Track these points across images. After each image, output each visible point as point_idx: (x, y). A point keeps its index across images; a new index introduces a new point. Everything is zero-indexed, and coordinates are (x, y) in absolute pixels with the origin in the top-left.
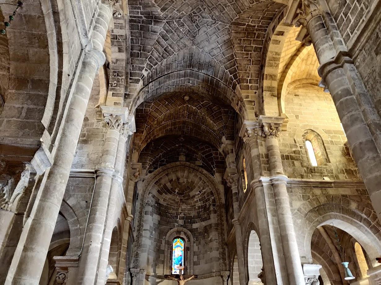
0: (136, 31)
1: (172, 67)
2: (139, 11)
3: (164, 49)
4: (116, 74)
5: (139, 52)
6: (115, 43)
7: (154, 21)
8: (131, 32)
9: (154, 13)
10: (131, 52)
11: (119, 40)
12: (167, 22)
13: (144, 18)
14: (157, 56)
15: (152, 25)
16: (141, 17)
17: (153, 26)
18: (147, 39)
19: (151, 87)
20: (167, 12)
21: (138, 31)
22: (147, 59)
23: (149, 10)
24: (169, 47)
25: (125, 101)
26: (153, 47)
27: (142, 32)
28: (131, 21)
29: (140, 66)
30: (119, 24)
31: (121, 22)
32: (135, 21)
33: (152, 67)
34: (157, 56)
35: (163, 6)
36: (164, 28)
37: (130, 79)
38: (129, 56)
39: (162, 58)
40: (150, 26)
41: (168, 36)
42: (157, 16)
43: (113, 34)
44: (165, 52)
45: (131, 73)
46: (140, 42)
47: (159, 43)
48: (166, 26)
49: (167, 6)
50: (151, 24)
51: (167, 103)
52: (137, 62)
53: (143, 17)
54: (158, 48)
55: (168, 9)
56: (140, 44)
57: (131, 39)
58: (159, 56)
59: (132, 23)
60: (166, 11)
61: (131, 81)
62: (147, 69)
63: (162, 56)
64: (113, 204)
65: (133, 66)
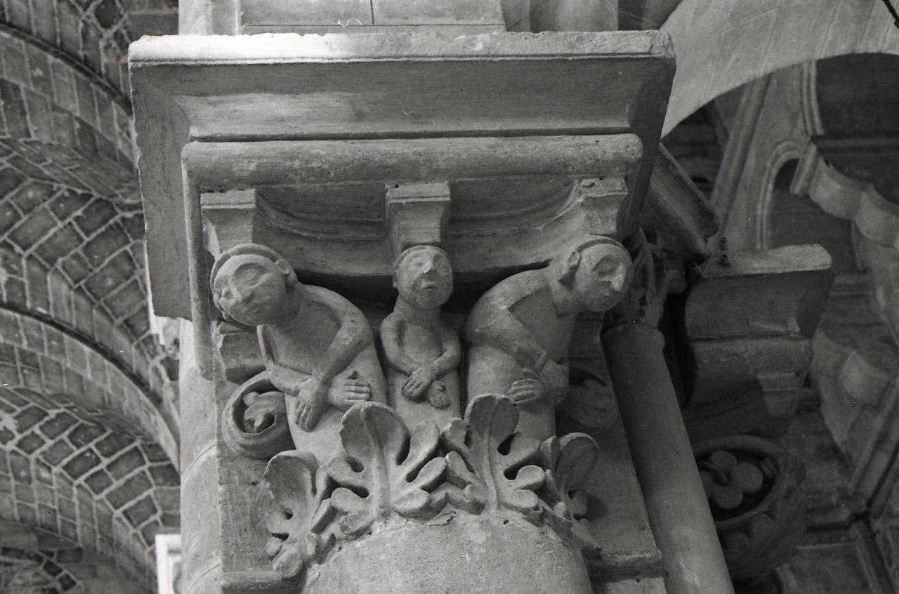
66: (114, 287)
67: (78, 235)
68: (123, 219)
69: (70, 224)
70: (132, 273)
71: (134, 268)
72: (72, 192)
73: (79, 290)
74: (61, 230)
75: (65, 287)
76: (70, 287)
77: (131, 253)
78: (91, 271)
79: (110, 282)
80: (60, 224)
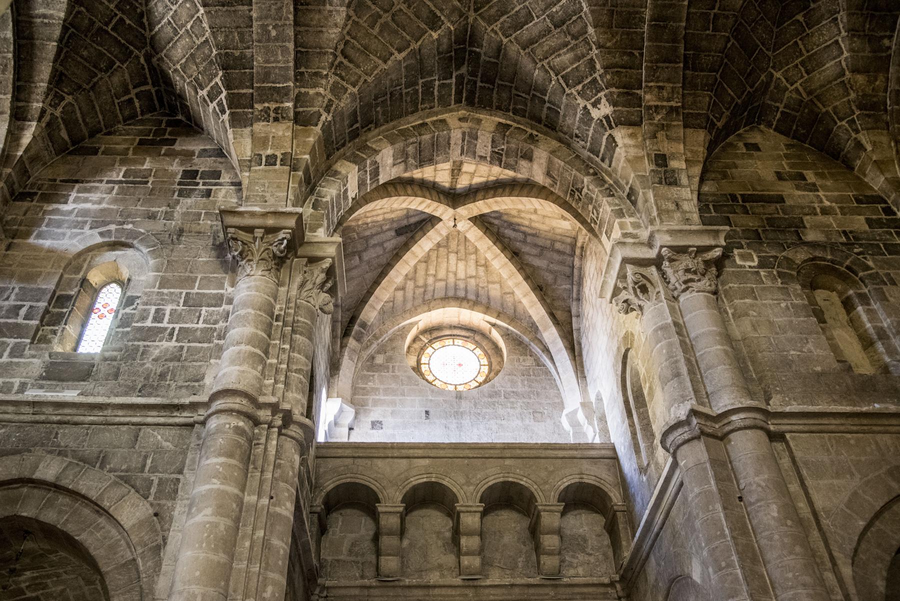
0: (495, 95)
1: (627, 5)
2: (437, 83)
3: (556, 27)
4: (577, 193)
5: (547, 105)
6: (511, 161)
7: (471, 45)
8: (499, 108)
9: (445, 47)
10: (545, 125)
11: (503, 150)
12: (476, 10)
13: (464, 70)
14: (570, 56)
15: (482, 52)
16: (460, 78)
17: (485, 50)
18: (515, 73)
19: (661, 99)
20: (441, 10)
21: (495, 92)
22: (568, 91)
23: (432, 62)
24: (554, 10)
25: (638, 211)
26: (539, 65)
27: (498, 81)
28: (471, 103)
29: (581, 119)
30: (463, 140)
31: (460, 136)
32: (471, 94)
33: (595, 80)
34: (570, 56)
35: (423, 26)
36: (491, 21)
37: (603, 160)
38: (553, 133)
39: (581, 39)
40: (483, 57)
41: (517, 9)
42: (453, 37)
43: (488, 159)
44: (564, 27)
45: (591, 150)
46: (523, 95)
47: (532, 42)
48: (486, 15)
49: (425, 13)
50: (478, 55)
51: (800, 17)
52: (569, 121)
53: (459, 72)
54: (546, 48)
55: (433, 8)
56: (527, 96)
57: (514, 114)
58: (572, 49)
59: (476, 100)
60: (439, 14)
61: (607, 161)
62: (593, 100)
63: (577, 39)
64: (758, 501)
65: (577, 136)
66: (82, 57)
67: (110, 21)
68: (137, 57)
69: (116, 15)
70: (101, 70)
71: (106, 71)
72: (142, 15)
73: (65, 29)
74: (108, 8)
75: (62, 15)
76: (65, 21)
77: (115, 67)
78: (86, 36)
79: (85, 53)
80: (112, 6)
